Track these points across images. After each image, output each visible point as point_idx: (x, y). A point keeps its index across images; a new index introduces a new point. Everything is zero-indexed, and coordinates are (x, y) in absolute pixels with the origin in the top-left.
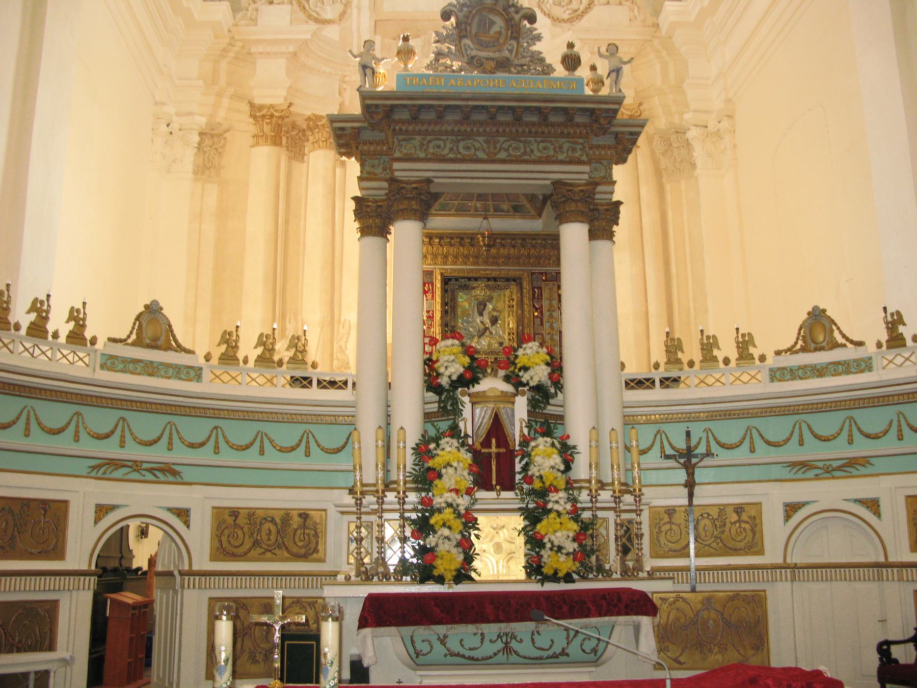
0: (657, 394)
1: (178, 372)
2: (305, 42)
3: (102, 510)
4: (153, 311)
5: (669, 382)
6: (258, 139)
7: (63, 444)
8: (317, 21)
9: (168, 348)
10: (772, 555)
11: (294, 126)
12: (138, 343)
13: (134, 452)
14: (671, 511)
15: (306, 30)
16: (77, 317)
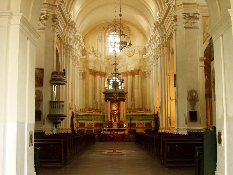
0: (129, 114)
5: (129, 113)
6: (90, 74)
8: (97, 57)
11: (95, 72)
14: (129, 123)
15: (96, 58)
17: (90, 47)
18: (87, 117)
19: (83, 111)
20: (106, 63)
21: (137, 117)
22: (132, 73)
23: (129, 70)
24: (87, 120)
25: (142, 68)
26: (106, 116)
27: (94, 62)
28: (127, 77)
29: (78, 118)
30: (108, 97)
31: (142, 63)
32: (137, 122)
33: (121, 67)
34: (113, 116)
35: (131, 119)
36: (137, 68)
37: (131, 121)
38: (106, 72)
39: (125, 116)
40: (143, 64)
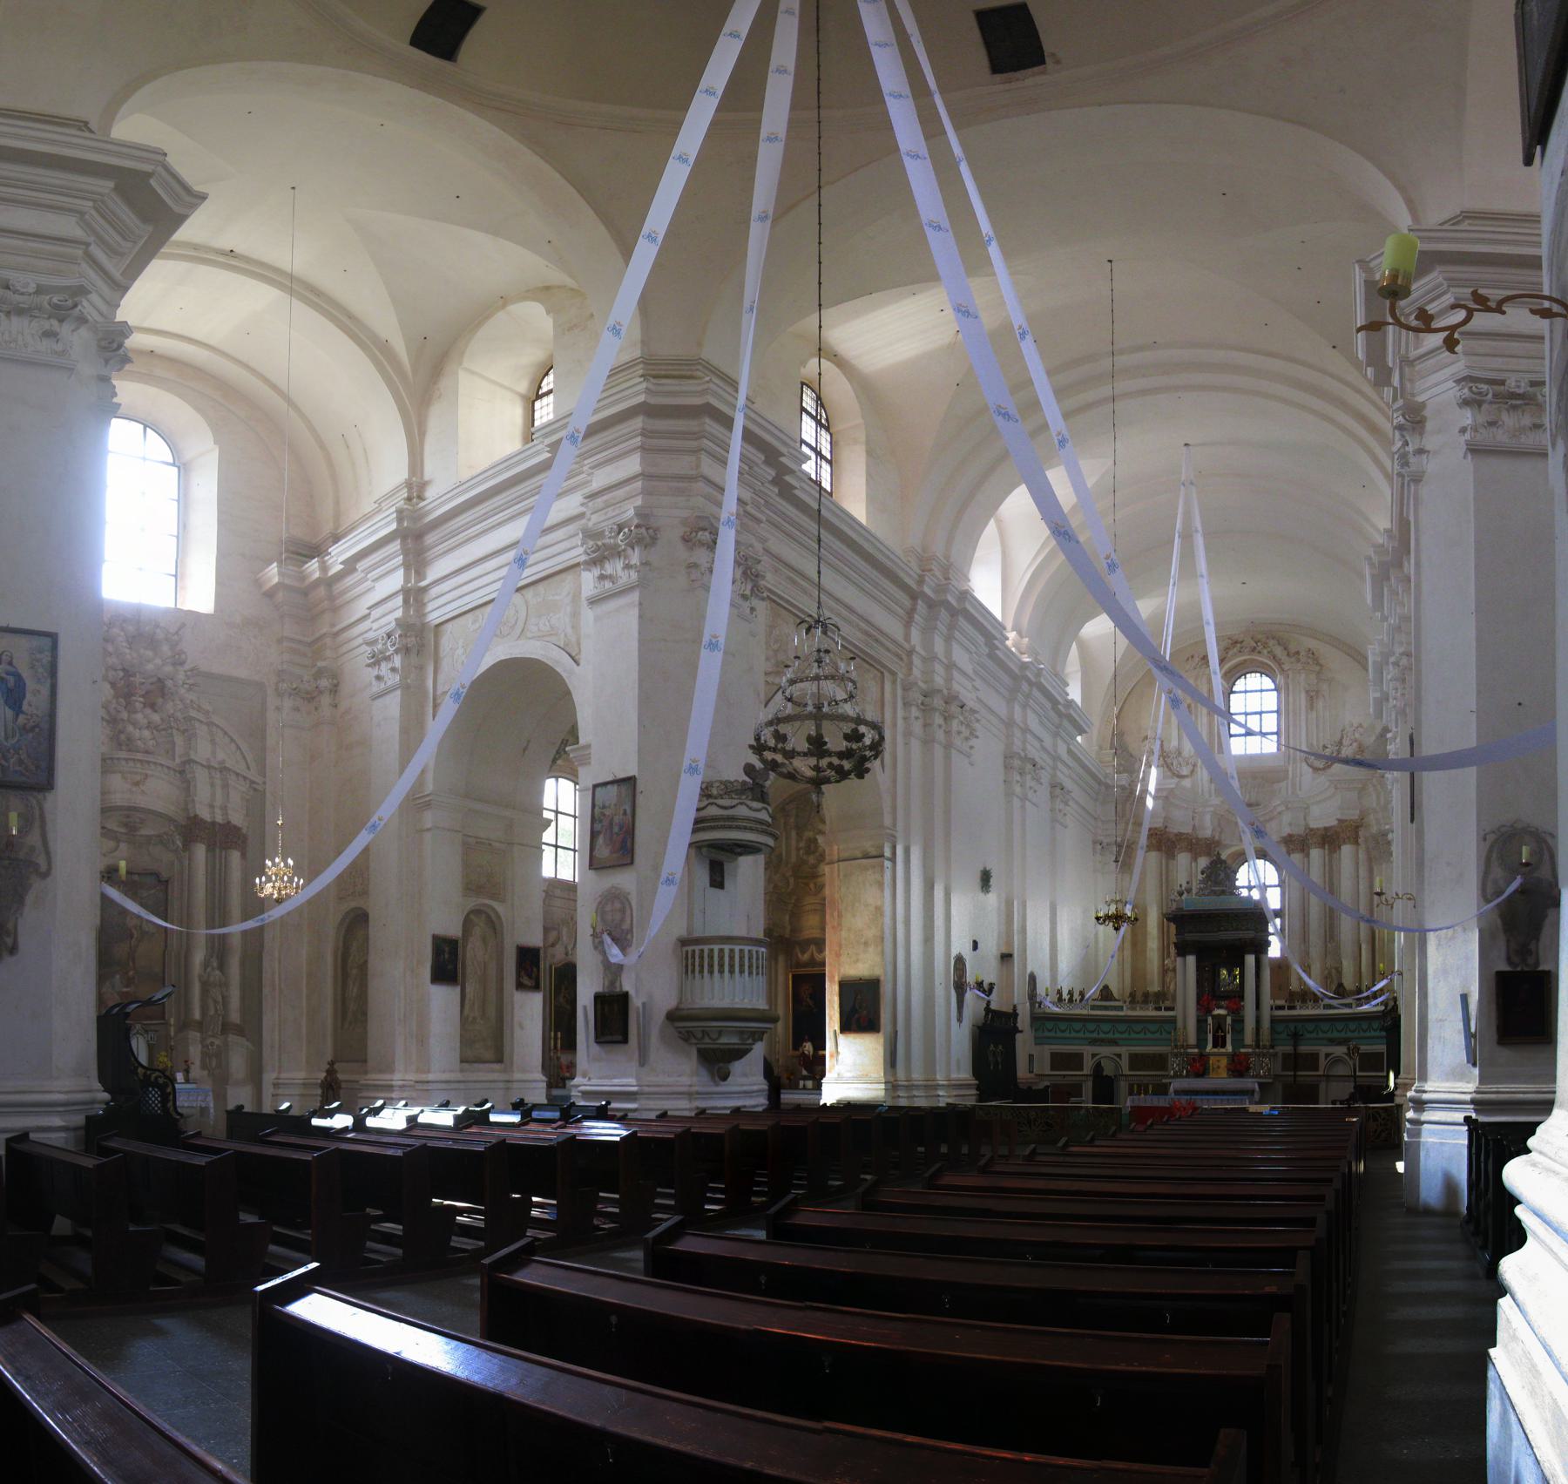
0: (1286, 1012)
1: (1116, 1008)
2: (1172, 790)
3: (1094, 1055)
4: (1106, 988)
5: (1291, 1008)
7: (1081, 1035)
9: (1111, 1000)
10: (1321, 1073)
12: (1101, 1000)
13: (1102, 1036)
14: (1289, 1054)
16: (1082, 994)
17: (1146, 738)
18: (1091, 1026)
19: (1071, 1000)
20: (1216, 801)
21: (1325, 1026)
22: (1330, 839)
23: (1313, 825)
24: (1094, 1042)
25: (1372, 817)
26: (1180, 1024)
27: (1166, 797)
28: (1308, 855)
29: (1047, 1034)
30: (1189, 937)
31: (1374, 797)
32: (1323, 1050)
33: (1280, 813)
34: (1210, 1020)
35: (1296, 1037)
36: (1353, 815)
37: (1295, 1046)
38: (1217, 838)
39: (1266, 1024)
40: (1378, 798)
